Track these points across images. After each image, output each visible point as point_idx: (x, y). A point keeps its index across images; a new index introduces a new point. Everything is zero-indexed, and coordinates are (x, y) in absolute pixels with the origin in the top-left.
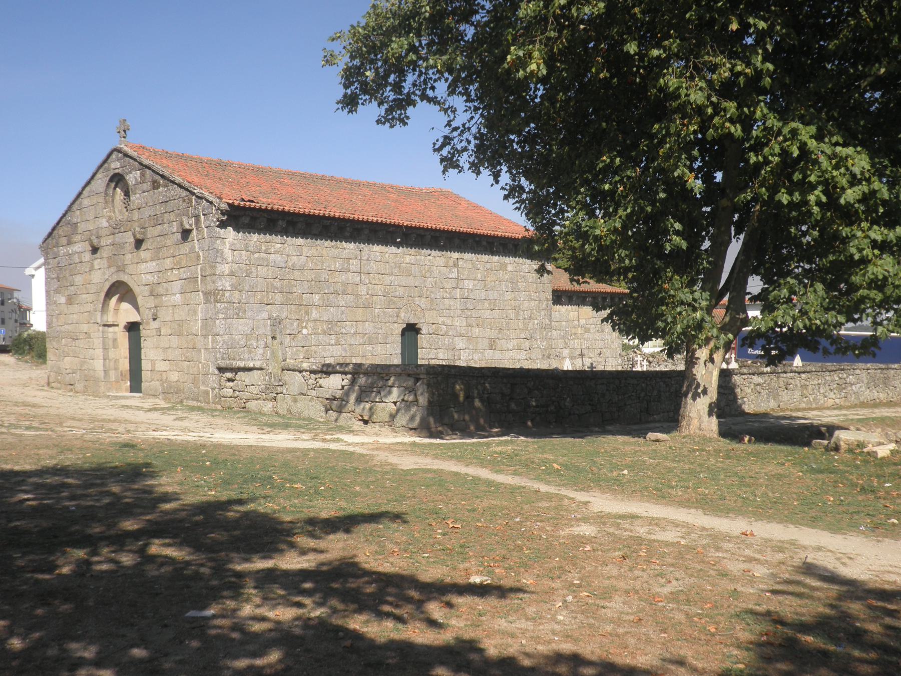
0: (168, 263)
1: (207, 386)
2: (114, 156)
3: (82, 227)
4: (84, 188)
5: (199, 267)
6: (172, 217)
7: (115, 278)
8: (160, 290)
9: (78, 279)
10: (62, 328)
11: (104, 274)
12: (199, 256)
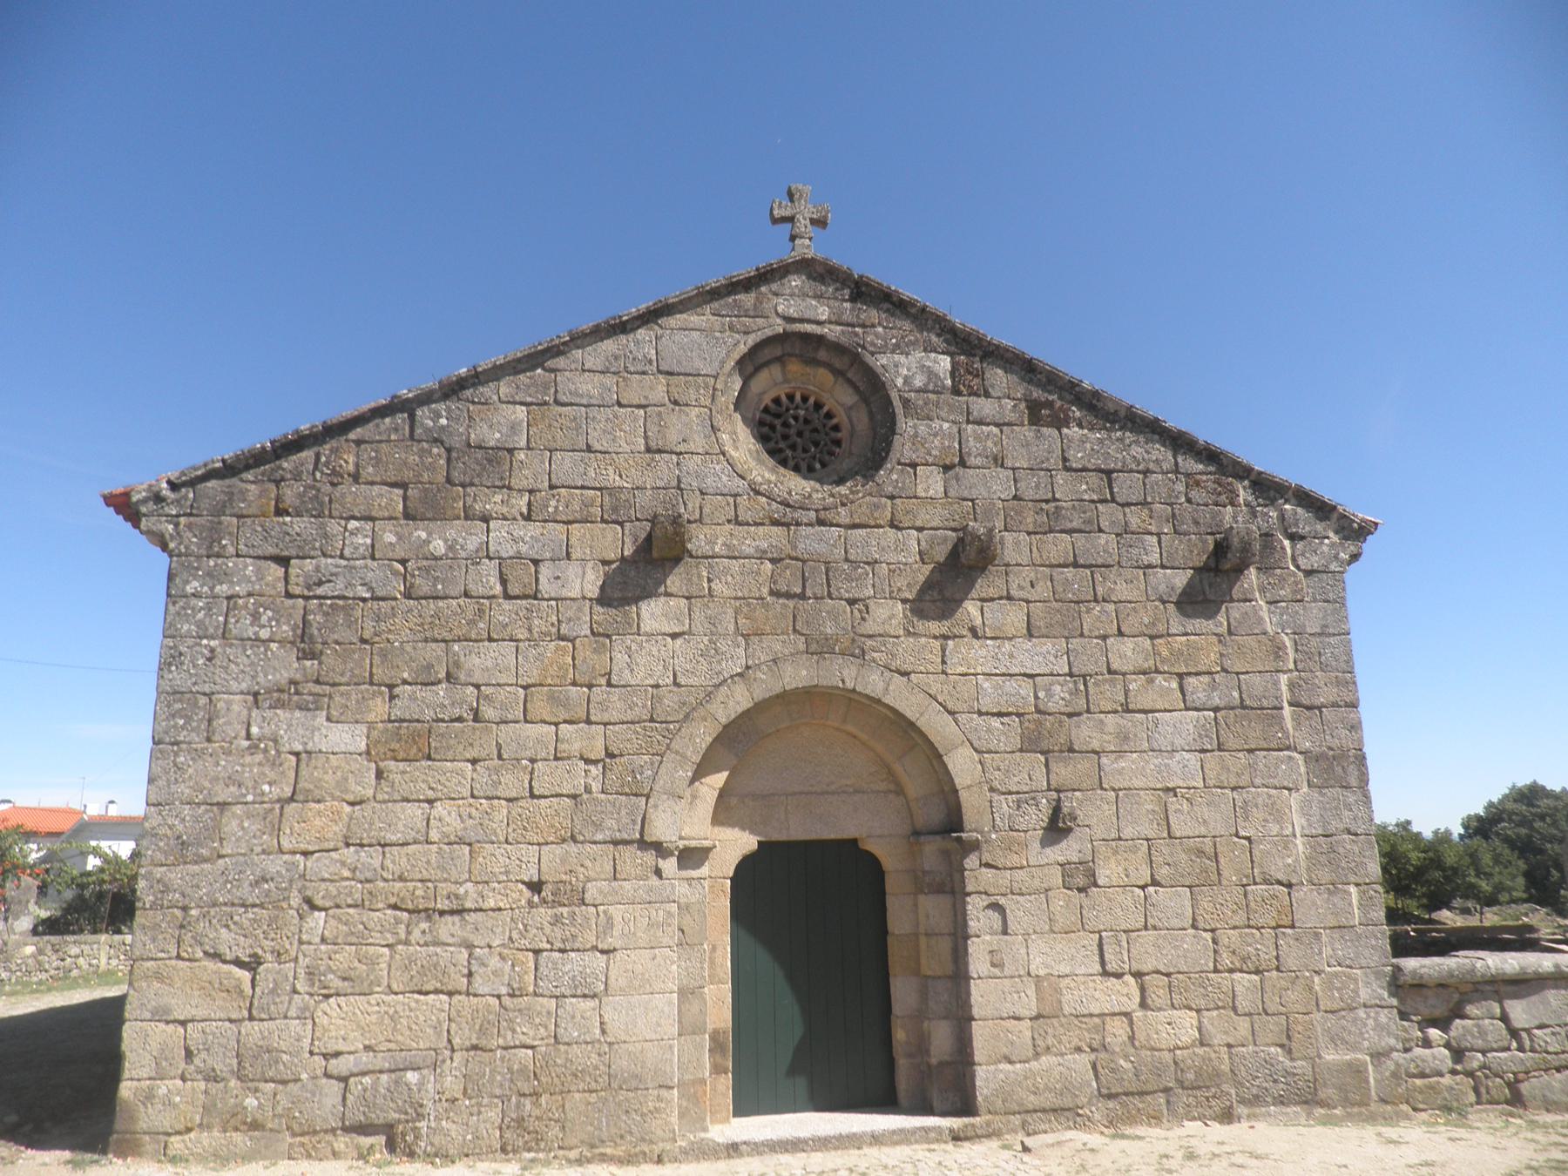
0: (1127, 653)
1: (1354, 1048)
2: (795, 281)
3: (529, 470)
4: (580, 339)
5: (1284, 678)
6: (1135, 518)
7: (798, 675)
8: (1085, 733)
9: (481, 661)
10: (319, 866)
11: (711, 653)
12: (1278, 651)
